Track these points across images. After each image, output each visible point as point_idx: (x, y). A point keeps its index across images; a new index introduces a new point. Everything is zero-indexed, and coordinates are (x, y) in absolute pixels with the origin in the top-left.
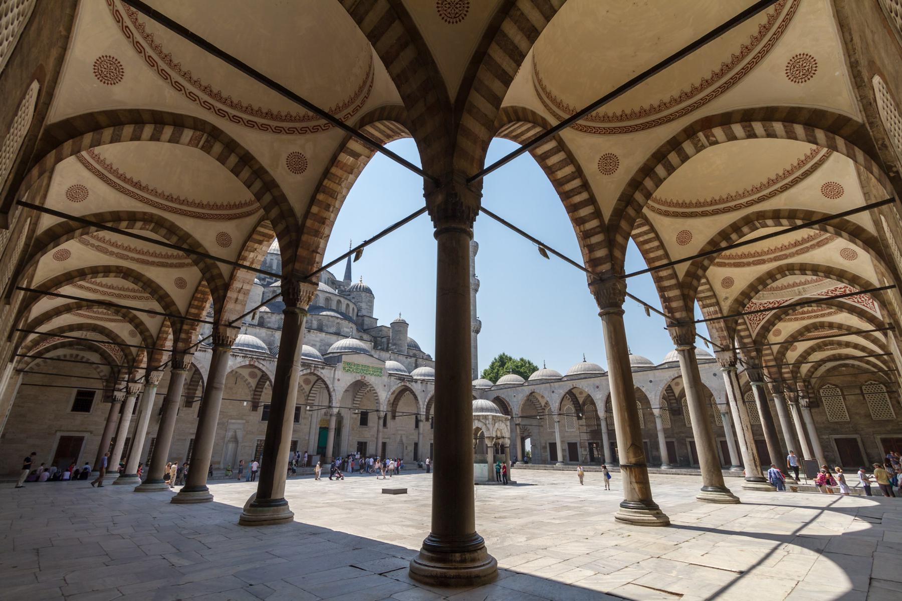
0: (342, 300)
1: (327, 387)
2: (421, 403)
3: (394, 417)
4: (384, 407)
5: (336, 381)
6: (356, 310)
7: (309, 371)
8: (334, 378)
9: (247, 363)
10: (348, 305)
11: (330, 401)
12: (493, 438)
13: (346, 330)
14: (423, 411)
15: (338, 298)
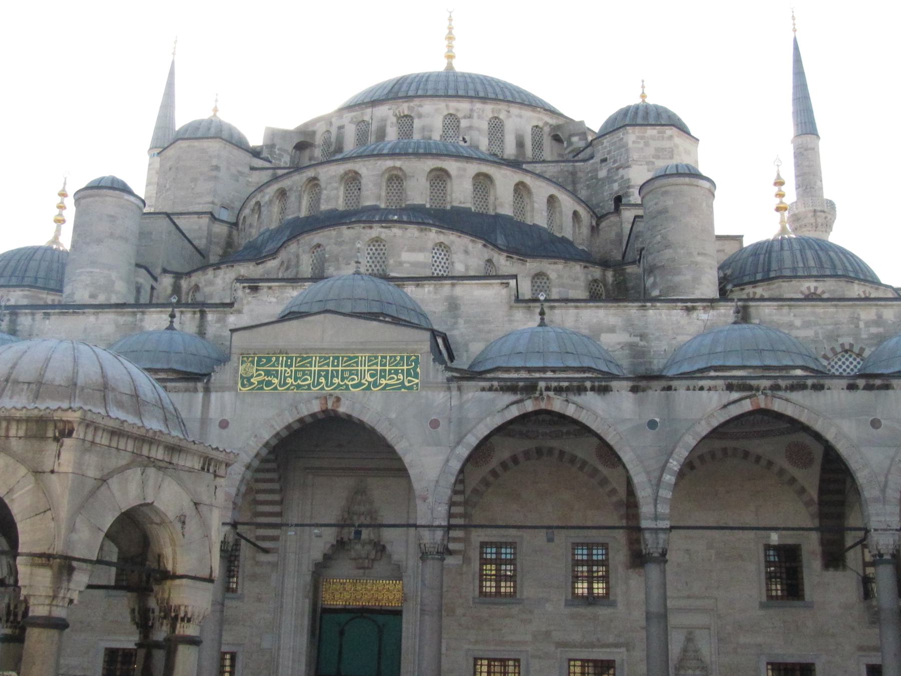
0: (451, 166)
5: (214, 429)
13: (406, 256)
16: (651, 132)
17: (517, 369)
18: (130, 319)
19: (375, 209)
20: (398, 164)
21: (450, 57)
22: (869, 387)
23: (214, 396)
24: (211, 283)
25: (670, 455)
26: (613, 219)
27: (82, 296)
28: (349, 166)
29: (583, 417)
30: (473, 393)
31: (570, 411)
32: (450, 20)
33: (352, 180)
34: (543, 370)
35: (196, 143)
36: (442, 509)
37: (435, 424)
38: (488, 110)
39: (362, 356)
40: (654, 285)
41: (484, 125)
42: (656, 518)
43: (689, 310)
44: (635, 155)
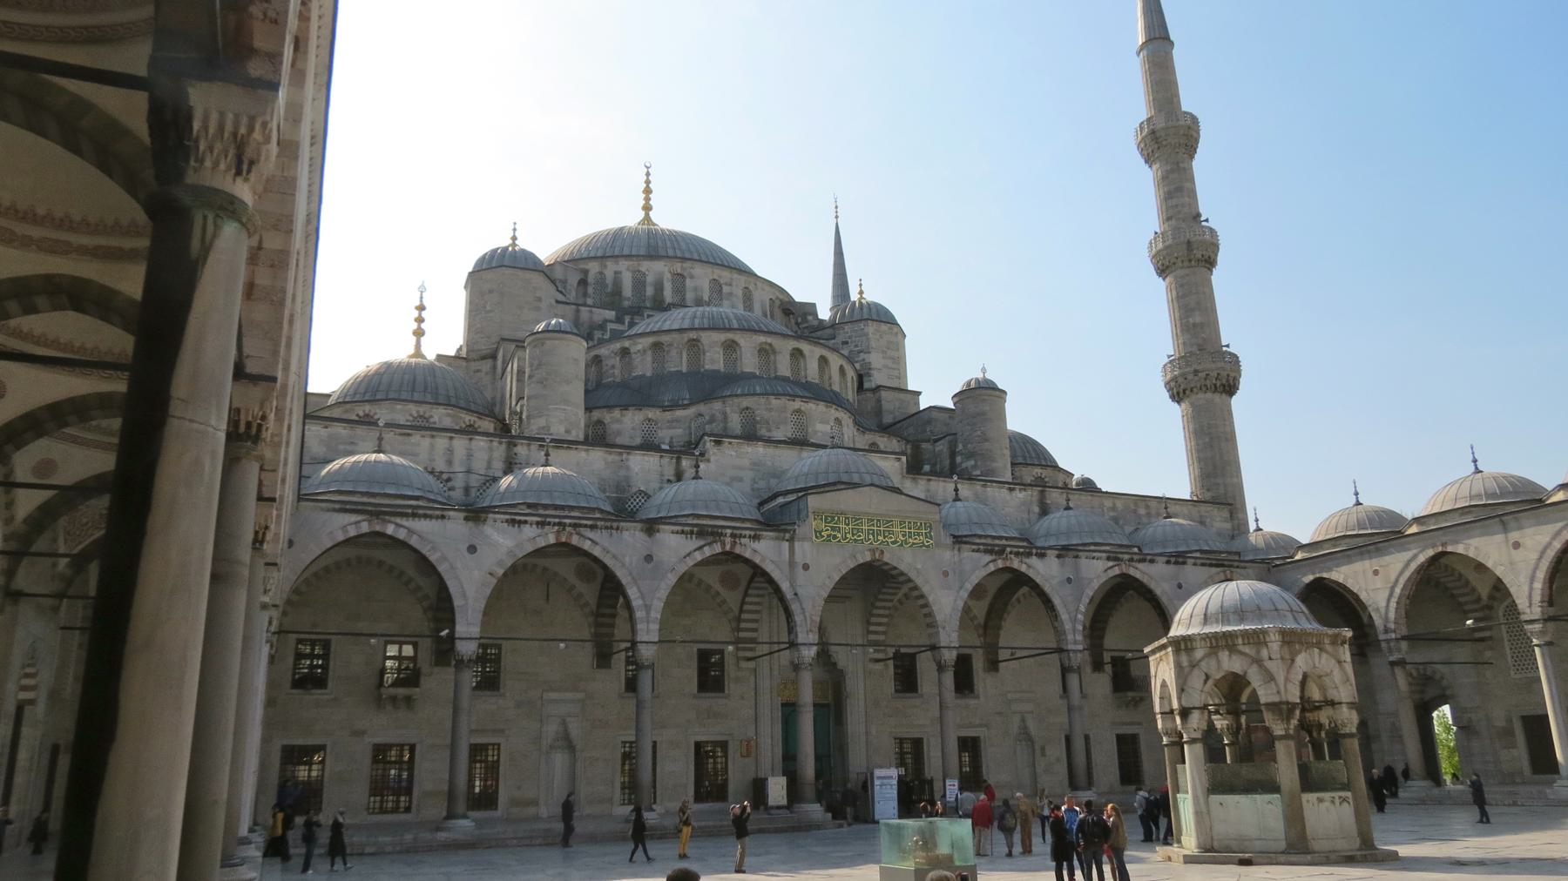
0: (805, 347)
1: (777, 590)
2: (1064, 616)
3: (993, 665)
4: (950, 637)
5: (800, 570)
6: (850, 373)
7: (717, 548)
8: (792, 563)
9: (552, 539)
10: (823, 361)
11: (791, 629)
12: (1291, 707)
13: (819, 427)
14: (1075, 639)
15: (793, 344)
16: (884, 327)
17: (986, 537)
18: (617, 458)
19: (752, 376)
20: (769, 340)
21: (647, 208)
22: (1176, 563)
23: (797, 544)
24: (618, 421)
25: (1080, 600)
26: (869, 395)
27: (558, 430)
28: (730, 335)
29: (1031, 574)
30: (967, 554)
31: (1023, 569)
32: (648, 174)
33: (731, 347)
34: (1000, 538)
35: (520, 273)
36: (955, 635)
37: (946, 574)
38: (741, 281)
39: (896, 520)
40: (975, 467)
41: (740, 293)
42: (1075, 642)
43: (1011, 490)
44: (873, 344)
